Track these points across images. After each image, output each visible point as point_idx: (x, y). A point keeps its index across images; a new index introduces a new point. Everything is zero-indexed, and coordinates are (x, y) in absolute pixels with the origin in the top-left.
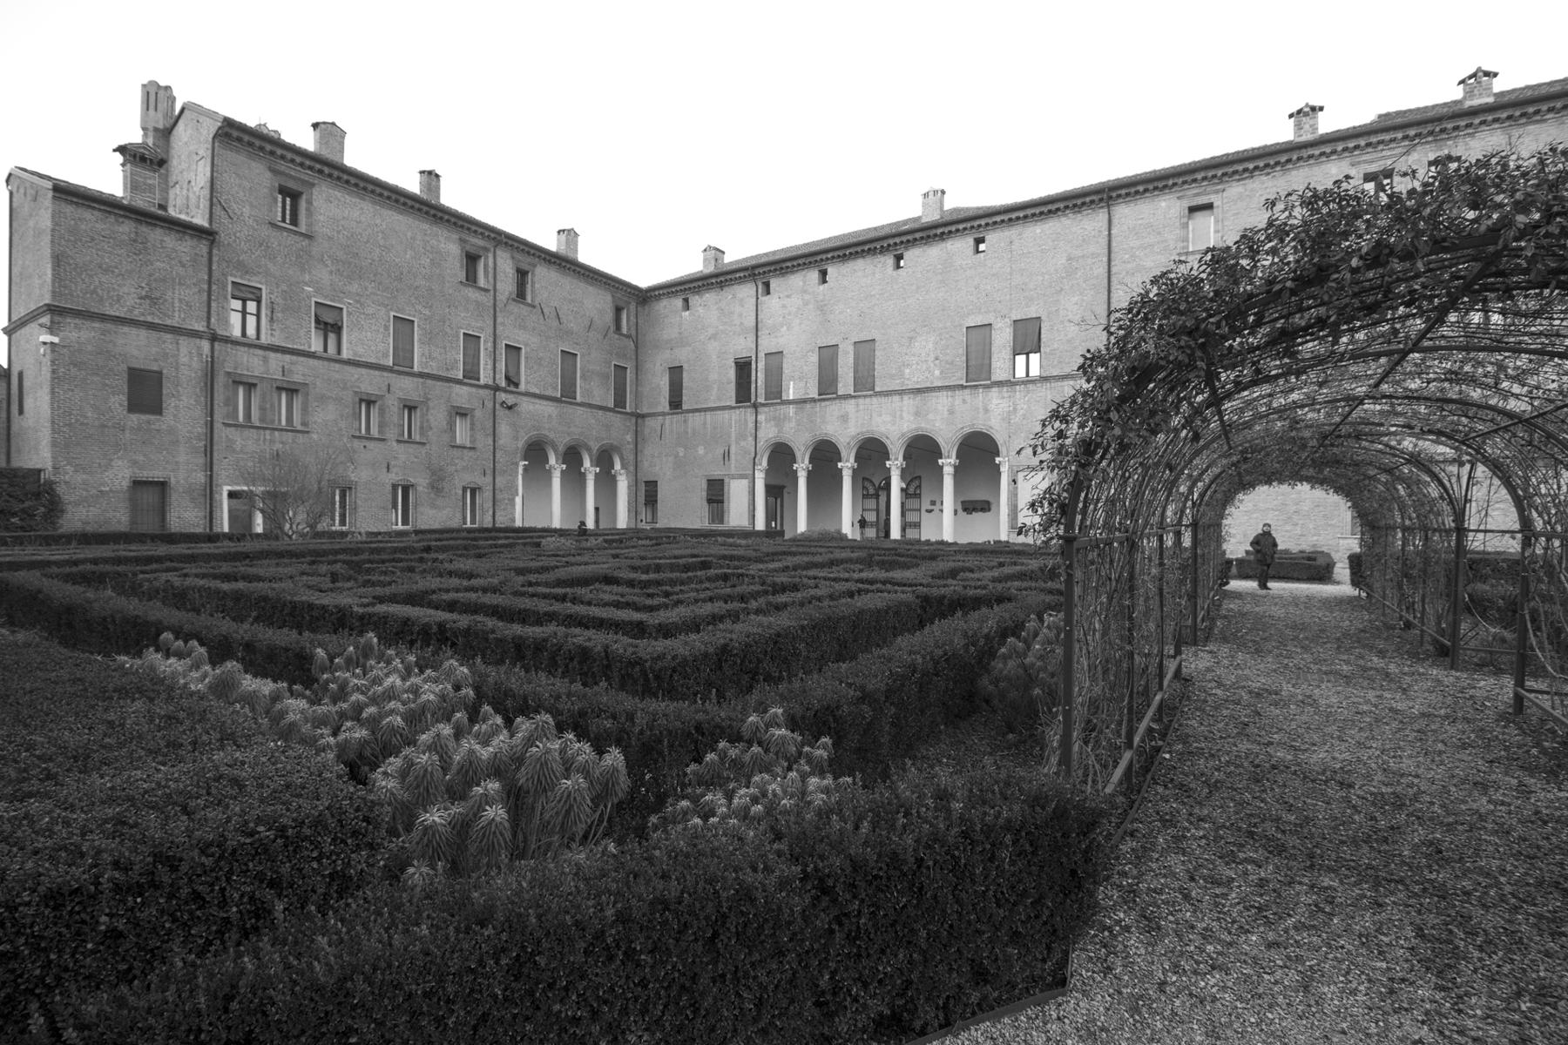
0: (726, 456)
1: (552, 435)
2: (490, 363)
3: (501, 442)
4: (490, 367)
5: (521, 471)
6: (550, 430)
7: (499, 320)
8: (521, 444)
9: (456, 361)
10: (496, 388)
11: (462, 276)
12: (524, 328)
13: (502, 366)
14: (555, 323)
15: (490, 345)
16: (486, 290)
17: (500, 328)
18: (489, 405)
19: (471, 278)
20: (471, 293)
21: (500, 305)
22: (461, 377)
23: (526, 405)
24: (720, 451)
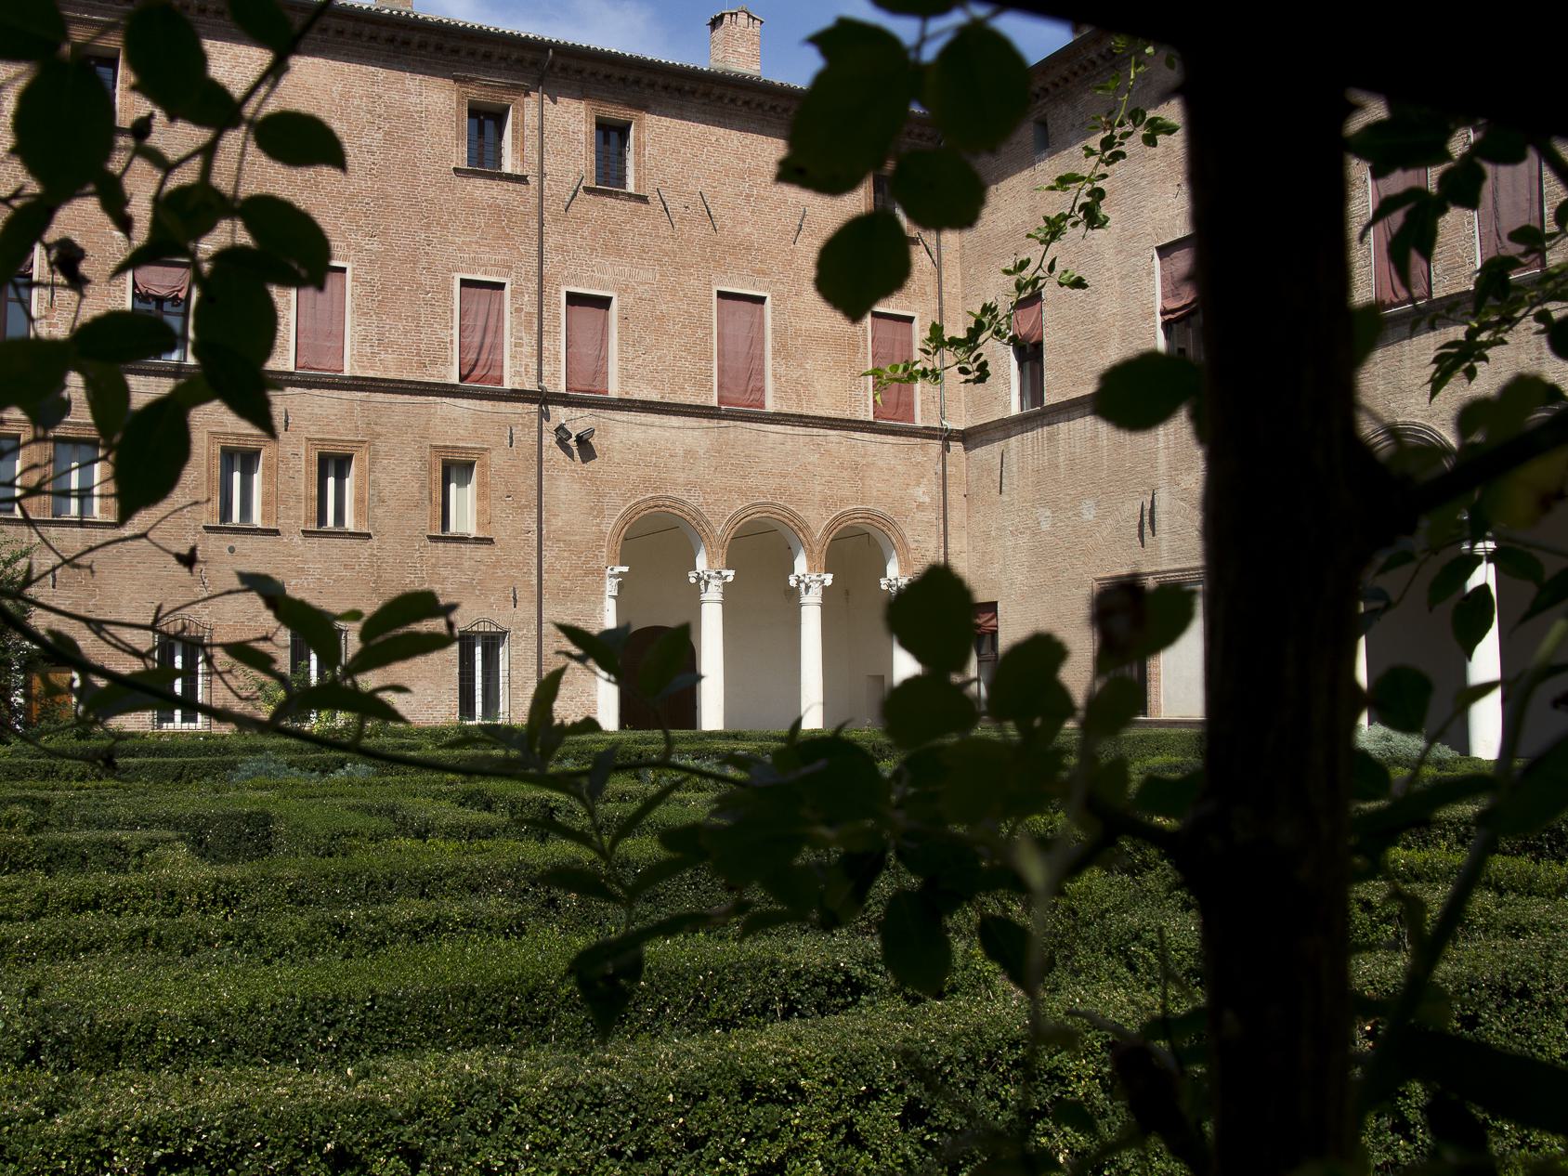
0: (1147, 521)
1: (694, 500)
2: (529, 341)
3: (554, 524)
4: (529, 348)
5: (611, 587)
6: (690, 486)
7: (550, 242)
8: (610, 524)
9: (444, 345)
10: (543, 399)
11: (459, 157)
12: (619, 251)
13: (557, 345)
14: (701, 231)
15: (529, 301)
16: (521, 179)
17: (552, 259)
18: (527, 438)
19: (483, 160)
20: (481, 189)
21: (552, 207)
22: (455, 379)
23: (618, 432)
24: (1131, 509)
